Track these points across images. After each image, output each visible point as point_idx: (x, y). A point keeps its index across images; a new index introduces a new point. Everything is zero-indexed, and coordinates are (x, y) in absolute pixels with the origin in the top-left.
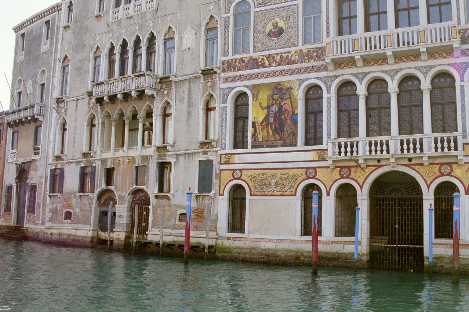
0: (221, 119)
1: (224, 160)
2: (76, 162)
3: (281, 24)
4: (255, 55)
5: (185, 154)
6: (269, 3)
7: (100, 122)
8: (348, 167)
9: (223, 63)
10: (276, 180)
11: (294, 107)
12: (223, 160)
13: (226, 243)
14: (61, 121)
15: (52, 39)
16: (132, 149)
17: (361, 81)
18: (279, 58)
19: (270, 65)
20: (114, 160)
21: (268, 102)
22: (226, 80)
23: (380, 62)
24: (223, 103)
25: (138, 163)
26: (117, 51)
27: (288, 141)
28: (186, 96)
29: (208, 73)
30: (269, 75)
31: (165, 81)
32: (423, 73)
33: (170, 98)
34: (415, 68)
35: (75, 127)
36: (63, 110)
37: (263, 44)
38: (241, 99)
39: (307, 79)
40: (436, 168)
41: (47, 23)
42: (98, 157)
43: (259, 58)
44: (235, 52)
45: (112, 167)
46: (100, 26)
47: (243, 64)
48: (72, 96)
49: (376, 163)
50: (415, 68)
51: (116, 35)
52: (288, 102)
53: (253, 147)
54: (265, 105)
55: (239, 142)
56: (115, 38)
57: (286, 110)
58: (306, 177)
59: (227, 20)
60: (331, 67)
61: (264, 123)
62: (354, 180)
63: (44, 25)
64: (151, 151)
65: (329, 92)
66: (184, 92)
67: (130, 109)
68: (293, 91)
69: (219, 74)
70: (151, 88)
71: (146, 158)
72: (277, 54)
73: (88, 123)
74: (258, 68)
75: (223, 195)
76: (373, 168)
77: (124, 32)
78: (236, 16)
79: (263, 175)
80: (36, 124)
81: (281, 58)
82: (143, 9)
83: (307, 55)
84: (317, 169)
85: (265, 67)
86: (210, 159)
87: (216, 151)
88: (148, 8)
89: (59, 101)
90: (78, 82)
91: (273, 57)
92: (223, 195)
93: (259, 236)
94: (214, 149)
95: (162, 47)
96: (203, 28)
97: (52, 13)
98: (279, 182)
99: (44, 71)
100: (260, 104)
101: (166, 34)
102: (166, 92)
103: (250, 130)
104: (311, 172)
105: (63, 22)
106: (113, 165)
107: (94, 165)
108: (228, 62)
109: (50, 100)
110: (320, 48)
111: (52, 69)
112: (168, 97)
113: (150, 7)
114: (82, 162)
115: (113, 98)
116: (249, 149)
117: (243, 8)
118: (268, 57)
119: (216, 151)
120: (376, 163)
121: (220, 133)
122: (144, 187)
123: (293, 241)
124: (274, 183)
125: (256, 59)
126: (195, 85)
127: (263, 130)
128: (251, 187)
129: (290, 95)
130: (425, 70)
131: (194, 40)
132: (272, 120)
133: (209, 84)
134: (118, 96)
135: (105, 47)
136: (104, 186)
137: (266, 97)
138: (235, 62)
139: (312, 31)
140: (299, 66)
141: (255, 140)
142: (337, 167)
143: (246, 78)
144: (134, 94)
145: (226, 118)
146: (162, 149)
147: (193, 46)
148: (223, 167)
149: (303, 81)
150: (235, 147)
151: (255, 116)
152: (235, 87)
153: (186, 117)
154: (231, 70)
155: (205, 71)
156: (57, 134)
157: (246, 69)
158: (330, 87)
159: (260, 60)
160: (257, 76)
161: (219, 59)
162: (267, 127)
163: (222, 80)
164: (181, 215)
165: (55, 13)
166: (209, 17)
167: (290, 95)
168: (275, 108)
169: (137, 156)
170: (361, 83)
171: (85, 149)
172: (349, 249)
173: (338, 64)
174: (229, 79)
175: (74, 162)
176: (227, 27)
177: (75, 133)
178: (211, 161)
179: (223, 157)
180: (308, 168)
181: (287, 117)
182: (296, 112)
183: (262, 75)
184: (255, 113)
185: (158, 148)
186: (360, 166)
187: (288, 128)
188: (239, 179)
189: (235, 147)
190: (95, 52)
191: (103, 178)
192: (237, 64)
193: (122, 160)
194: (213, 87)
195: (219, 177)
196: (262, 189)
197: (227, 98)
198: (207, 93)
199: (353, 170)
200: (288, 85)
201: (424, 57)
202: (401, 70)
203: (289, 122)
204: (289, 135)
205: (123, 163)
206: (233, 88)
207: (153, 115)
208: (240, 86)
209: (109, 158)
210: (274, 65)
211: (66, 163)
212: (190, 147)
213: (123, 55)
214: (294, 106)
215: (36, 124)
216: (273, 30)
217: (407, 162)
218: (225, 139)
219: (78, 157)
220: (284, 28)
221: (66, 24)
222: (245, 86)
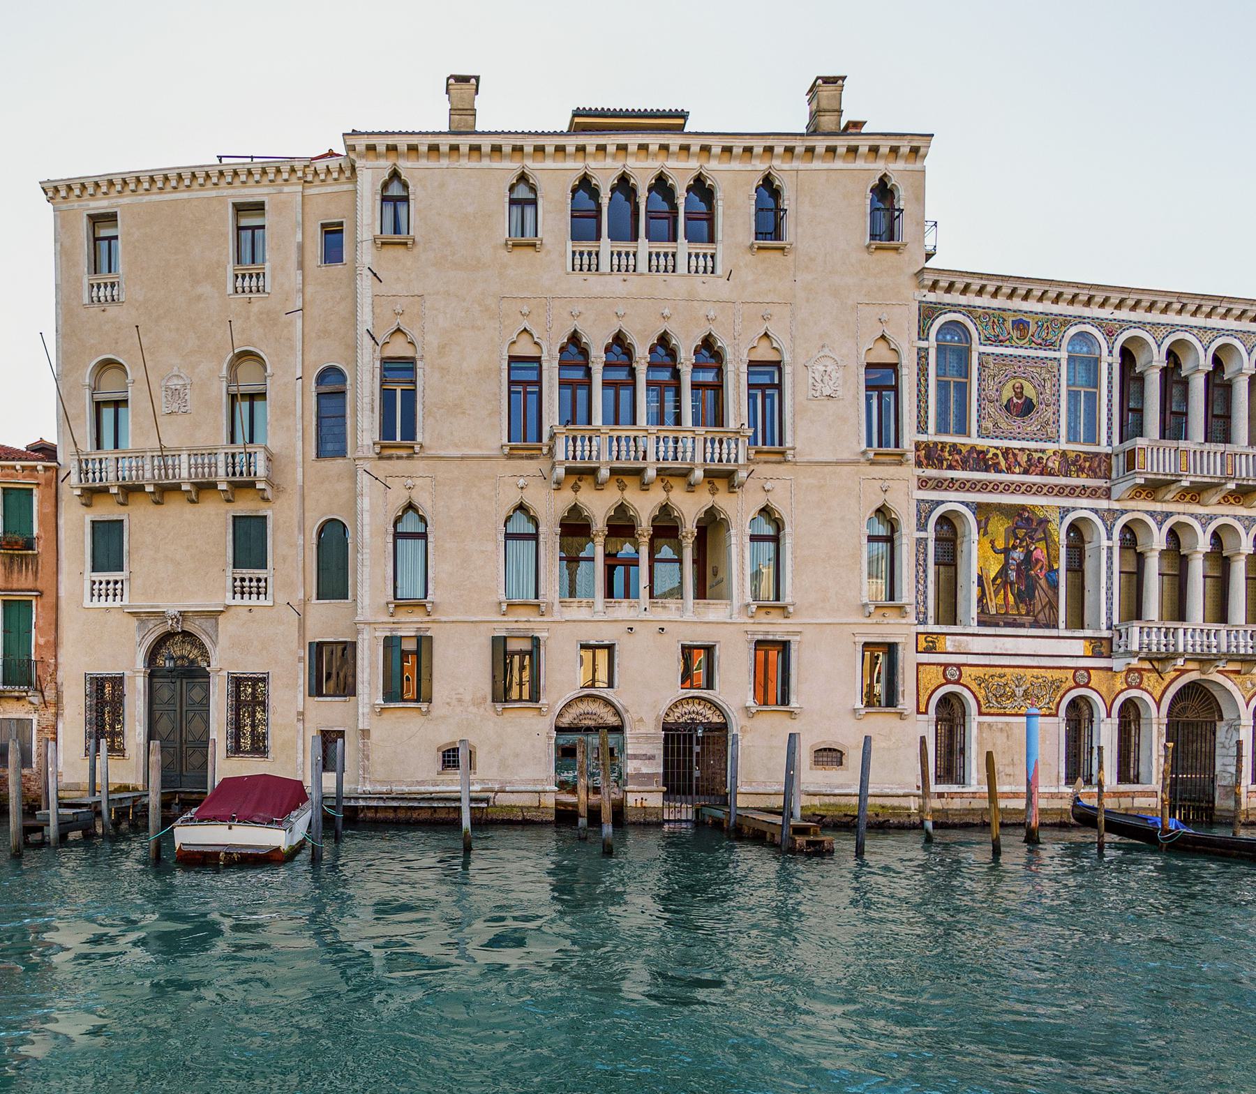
1: (925, 644)
3: (1029, 392)
6: (1007, 343)
9: (918, 446)
10: (1024, 687)
11: (1052, 558)
12: (923, 645)
17: (1160, 524)
18: (1025, 458)
19: (1009, 470)
30: (1007, 488)
34: (1235, 517)
37: (995, 425)
39: (1074, 509)
44: (942, 428)
47: (957, 457)
50: (1235, 517)
52: (1042, 545)
53: (980, 623)
54: (1000, 544)
57: (1037, 560)
58: (1073, 684)
61: (999, 581)
62: (1146, 690)
72: (1022, 450)
74: (986, 470)
75: (926, 713)
78: (940, 349)
79: (1000, 676)
81: (1029, 460)
84: (1092, 672)
85: (1001, 471)
91: (1015, 455)
92: (926, 713)
100: (992, 542)
104: (1082, 676)
108: (927, 446)
110: (1097, 454)
118: (1006, 452)
127: (997, 593)
128: (981, 699)
129: (1044, 532)
130: (1247, 523)
132: (1013, 575)
137: (1002, 529)
138: (942, 450)
140: (1062, 481)
141: (982, 611)
143: (963, 486)
152: (943, 502)
154: (934, 466)
157: (963, 469)
159: (990, 455)
160: (984, 487)
168: (1018, 554)
172: (1140, 802)
179: (922, 638)
180: (1077, 669)
181: (1038, 572)
183: (995, 487)
188: (957, 682)
197: (927, 520)
199: (1146, 675)
203: (1043, 582)
204: (1044, 607)
208: (953, 501)
210: (1017, 470)
214: (1053, 553)
216: (1015, 400)
220: (1035, 401)
222: (962, 503)
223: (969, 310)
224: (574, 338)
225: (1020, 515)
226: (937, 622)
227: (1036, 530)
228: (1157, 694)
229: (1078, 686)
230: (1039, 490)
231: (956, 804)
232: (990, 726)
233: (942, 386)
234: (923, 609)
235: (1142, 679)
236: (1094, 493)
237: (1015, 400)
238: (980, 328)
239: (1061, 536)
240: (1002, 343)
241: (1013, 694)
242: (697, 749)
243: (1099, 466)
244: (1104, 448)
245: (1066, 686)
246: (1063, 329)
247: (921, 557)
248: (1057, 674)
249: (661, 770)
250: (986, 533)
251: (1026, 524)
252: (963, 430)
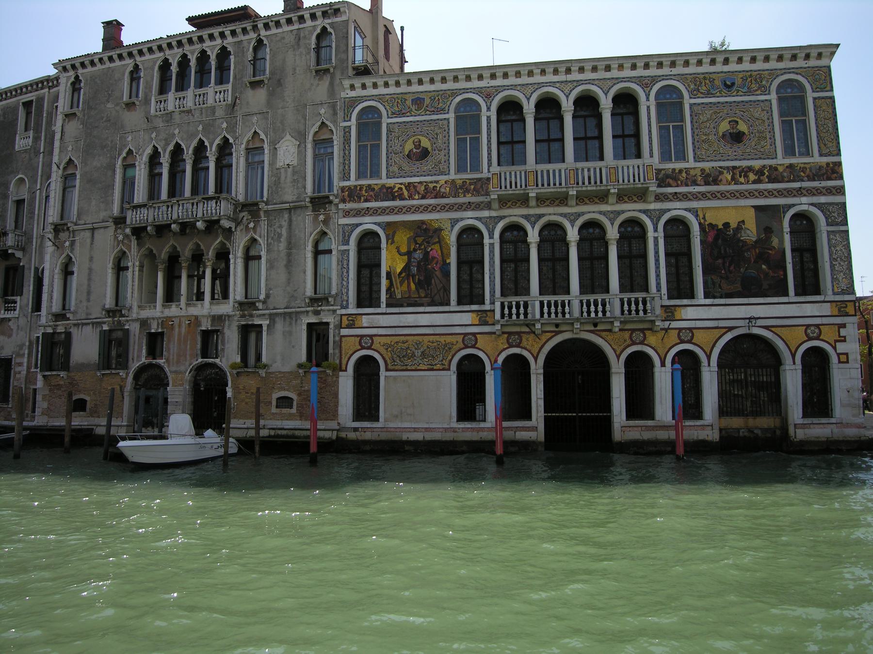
0: (340, 267)
1: (347, 322)
2: (93, 324)
3: (425, 143)
4: (391, 182)
5: (285, 313)
7: (137, 263)
8: (519, 334)
9: (343, 189)
11: (445, 255)
13: (352, 436)
14: (62, 259)
15: (37, 131)
16: (195, 305)
18: (423, 188)
19: (411, 197)
20: (165, 322)
21: (409, 247)
22: (347, 214)
23: (557, 202)
24: (343, 245)
25: (206, 325)
26: (165, 160)
27: (437, 298)
28: (284, 232)
29: (320, 202)
30: (409, 210)
31: (251, 208)
32: (610, 220)
33: (258, 233)
34: (600, 213)
35: (90, 269)
36: (67, 244)
37: (400, 168)
38: (366, 240)
39: (462, 219)
40: (627, 335)
41: (28, 105)
42: (134, 316)
43: (395, 187)
44: (360, 175)
45: (160, 330)
46: (134, 119)
47: (371, 193)
48: (83, 222)
49: (554, 329)
50: (600, 213)
51: (163, 136)
52: (437, 247)
53: (388, 305)
54: (404, 249)
55: (367, 297)
56: (161, 140)
57: (434, 258)
58: (462, 346)
59: (347, 131)
60: (495, 205)
61: (404, 274)
62: (525, 349)
63: (21, 108)
64: (225, 308)
65: (491, 237)
66: (281, 227)
67: (190, 246)
68: (444, 233)
69: (337, 205)
70: (228, 218)
71: (218, 319)
72: (421, 183)
73: (114, 264)
74: (393, 200)
75: (346, 370)
76: (549, 335)
77: (176, 132)
78: (359, 126)
79: (404, 342)
80: (8, 263)
81: (426, 189)
82: (210, 101)
83: (461, 188)
84: (478, 336)
86: (324, 321)
87: (334, 311)
88: (218, 100)
89: (58, 229)
90: (94, 203)
91: (415, 187)
92: (346, 370)
93: (400, 425)
94: (331, 308)
95: (242, 160)
96: (310, 138)
97: (37, 90)
98: (427, 352)
99: (22, 180)
100: (398, 248)
101: (248, 142)
102: (252, 225)
103: (384, 282)
104: (470, 340)
105: (63, 105)
106: (162, 328)
107: (127, 327)
109: (35, 226)
110: (480, 179)
111: (39, 177)
112: (255, 233)
113: (222, 100)
114: (104, 323)
115: (162, 229)
116: (383, 308)
118: (409, 186)
119: (334, 311)
120: (554, 329)
121: (340, 286)
122: (217, 361)
123: (446, 429)
124: (420, 354)
125: (390, 188)
126: (300, 218)
127: (401, 283)
128: (387, 359)
129: (439, 238)
130: (612, 216)
131: (296, 155)
132: (414, 270)
133: (322, 217)
134: (173, 226)
135: (144, 151)
136: (143, 360)
137: (405, 239)
138: (361, 189)
139: (468, 157)
141: (391, 296)
142: (504, 333)
143: (375, 212)
144: (200, 225)
145: (348, 265)
146: (247, 305)
147: (295, 162)
148: (344, 332)
149: (457, 221)
150: (359, 305)
151: (390, 263)
152: (361, 224)
153: (285, 262)
154: (354, 201)
155: (315, 198)
156: (56, 281)
158: (493, 231)
159: (396, 189)
160: (392, 211)
161: (335, 184)
162: (408, 279)
163: (341, 214)
164: (278, 399)
165: (43, 91)
166: (319, 123)
167: (439, 238)
168: (418, 255)
169: (203, 316)
170: (533, 228)
171: (109, 302)
173: (504, 202)
175: (88, 324)
176: (347, 141)
177: (89, 279)
178: (327, 324)
179: (345, 318)
180: (465, 334)
182: (448, 261)
183: (400, 210)
184: (390, 260)
185: (241, 304)
186: (534, 333)
187: (437, 282)
188: (369, 348)
189: (359, 305)
190: (125, 158)
191: (144, 347)
192: (364, 192)
193: (177, 321)
194: (326, 222)
195: (339, 345)
196: (402, 362)
197: (349, 238)
198: (318, 230)
199: (524, 337)
200: (436, 226)
201: (612, 199)
202: (583, 214)
203: (438, 273)
204: (439, 291)
205: (180, 326)
206: (358, 225)
207: (231, 256)
208: (369, 223)
209: (153, 319)
210: (417, 197)
211: (75, 325)
212: (293, 304)
213: (176, 168)
214: (445, 251)
215: (8, 263)
216: (415, 150)
217: (592, 328)
218: (347, 293)
219: (99, 316)
220: (430, 149)
221: (67, 110)
223: (380, 98)
225: (419, 227)
227: (432, 237)
228: (535, 351)
229: (466, 347)
230: (433, 209)
231: (368, 436)
232: (395, 378)
233: (361, 149)
234: (346, 298)
235: (521, 340)
236: (478, 207)
237: (415, 150)
238: (388, 107)
239: (452, 239)
240: (403, 115)
241: (413, 355)
243: (482, 187)
244: (485, 174)
245: (456, 348)
246: (451, 99)
247: (345, 262)
248: (449, 339)
250: (393, 242)
251: (425, 233)
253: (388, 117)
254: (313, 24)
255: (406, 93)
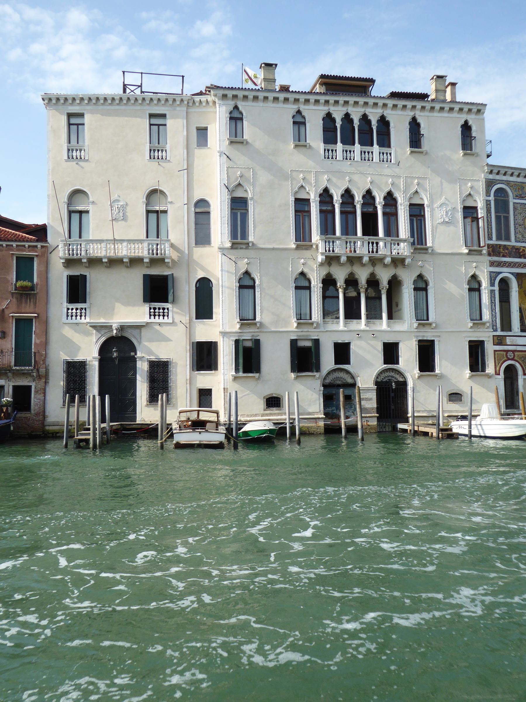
9: (489, 246)
24: (491, 286)
44: (499, 238)
47: (506, 251)
74: (520, 258)
75: (499, 374)
78: (496, 201)
92: (499, 374)
117: (499, 195)
125: (518, 249)
145: (495, 300)
152: (501, 273)
157: (510, 257)
159: (521, 250)
174: (495, 263)
188: (513, 359)
192: (502, 250)
197: (494, 281)
208: (506, 272)
218: (496, 321)
223: (508, 183)
224: (326, 190)
226: (502, 330)
233: (498, 218)
242: (392, 395)
249: (375, 406)
252: (508, 239)
253: (514, 198)
254: (459, 116)
255: (523, 183)
